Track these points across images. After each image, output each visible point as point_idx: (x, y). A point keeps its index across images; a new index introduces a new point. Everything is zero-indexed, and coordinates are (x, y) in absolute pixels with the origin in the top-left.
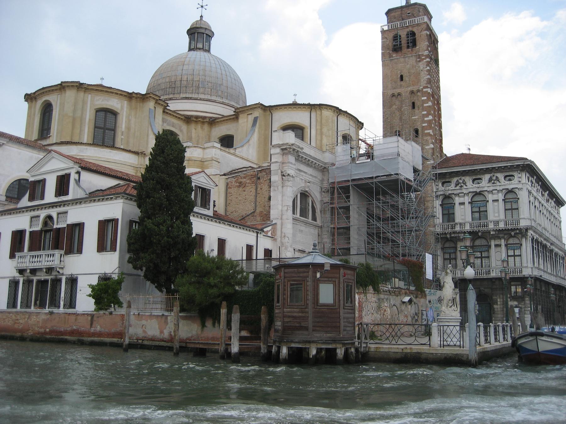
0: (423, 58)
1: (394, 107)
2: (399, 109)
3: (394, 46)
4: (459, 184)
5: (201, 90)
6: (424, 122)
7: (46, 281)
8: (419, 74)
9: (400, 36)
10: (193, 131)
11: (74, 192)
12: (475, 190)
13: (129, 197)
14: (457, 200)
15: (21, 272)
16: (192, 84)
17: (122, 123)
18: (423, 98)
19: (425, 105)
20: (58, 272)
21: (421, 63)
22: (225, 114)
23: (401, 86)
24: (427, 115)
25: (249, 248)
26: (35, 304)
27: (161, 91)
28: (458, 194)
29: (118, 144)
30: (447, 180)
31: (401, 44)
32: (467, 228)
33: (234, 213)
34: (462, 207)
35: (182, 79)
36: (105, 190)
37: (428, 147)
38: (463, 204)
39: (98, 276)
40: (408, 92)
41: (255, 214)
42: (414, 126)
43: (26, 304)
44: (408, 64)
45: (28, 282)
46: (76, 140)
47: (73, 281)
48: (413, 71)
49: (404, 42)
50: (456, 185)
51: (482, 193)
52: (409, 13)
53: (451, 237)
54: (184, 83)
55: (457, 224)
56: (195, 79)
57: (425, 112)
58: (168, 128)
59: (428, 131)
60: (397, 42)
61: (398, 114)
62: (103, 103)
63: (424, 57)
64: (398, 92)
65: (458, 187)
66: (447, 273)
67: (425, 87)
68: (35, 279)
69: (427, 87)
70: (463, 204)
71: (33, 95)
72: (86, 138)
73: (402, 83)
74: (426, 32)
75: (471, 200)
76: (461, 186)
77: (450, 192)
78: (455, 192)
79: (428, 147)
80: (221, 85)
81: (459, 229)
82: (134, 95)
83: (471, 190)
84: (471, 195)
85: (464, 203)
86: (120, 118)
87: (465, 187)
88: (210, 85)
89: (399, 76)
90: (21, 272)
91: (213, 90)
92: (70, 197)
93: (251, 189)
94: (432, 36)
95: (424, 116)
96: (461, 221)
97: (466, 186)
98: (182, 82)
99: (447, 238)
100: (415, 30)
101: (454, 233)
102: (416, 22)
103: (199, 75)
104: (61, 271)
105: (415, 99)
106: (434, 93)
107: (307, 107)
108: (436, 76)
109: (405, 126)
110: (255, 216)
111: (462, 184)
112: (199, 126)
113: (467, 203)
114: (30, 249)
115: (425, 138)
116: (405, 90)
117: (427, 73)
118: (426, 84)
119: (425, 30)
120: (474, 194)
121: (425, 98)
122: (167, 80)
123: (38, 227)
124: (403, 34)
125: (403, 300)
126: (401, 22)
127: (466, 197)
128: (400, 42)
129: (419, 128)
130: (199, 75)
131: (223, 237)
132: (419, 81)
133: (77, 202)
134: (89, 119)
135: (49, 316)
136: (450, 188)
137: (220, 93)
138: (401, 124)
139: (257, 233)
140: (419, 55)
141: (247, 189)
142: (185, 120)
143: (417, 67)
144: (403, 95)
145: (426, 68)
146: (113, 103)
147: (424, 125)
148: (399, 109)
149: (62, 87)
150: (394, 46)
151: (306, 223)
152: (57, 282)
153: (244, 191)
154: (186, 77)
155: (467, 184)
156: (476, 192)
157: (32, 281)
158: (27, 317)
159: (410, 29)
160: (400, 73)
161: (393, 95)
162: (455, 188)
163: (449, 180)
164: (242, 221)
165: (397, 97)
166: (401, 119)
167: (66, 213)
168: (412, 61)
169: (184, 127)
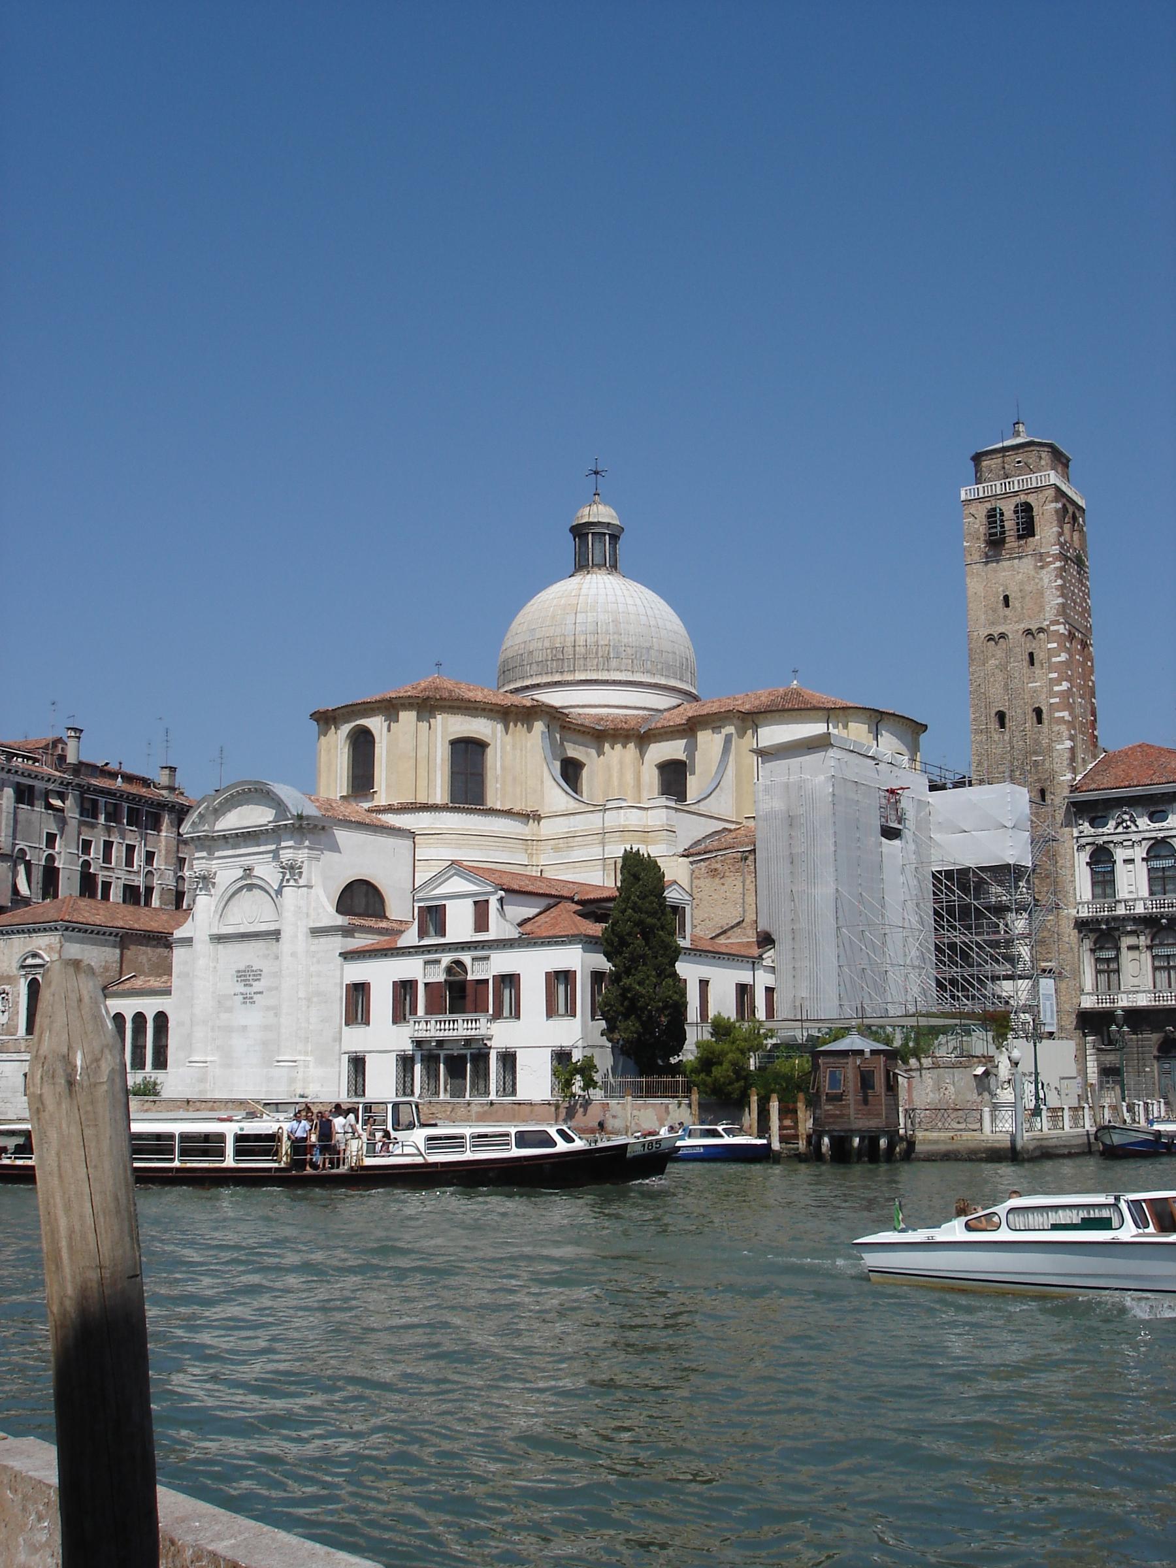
0: (1048, 560)
1: (992, 662)
3: (991, 535)
4: (1122, 823)
5: (614, 663)
6: (1052, 694)
7: (465, 1056)
8: (1042, 594)
9: (1002, 514)
11: (498, 928)
12: (1154, 834)
13: (590, 943)
14: (1120, 854)
15: (418, 1043)
16: (597, 653)
17: (495, 761)
18: (1050, 646)
19: (1054, 660)
20: (486, 1044)
21: (1044, 571)
22: (661, 708)
23: (1005, 617)
24: (1058, 682)
26: (446, 1089)
27: (534, 667)
28: (1122, 843)
29: (493, 799)
30: (1099, 814)
31: (1003, 533)
32: (1140, 909)
33: (707, 921)
34: (1130, 867)
35: (577, 644)
36: (533, 918)
37: (1063, 746)
38: (1130, 861)
39: (550, 1049)
40: (1021, 632)
41: (744, 925)
42: (1034, 703)
44: (1018, 573)
46: (422, 799)
47: (508, 1060)
48: (1028, 588)
49: (1009, 525)
50: (1118, 824)
51: (1168, 840)
52: (1019, 462)
53: (1108, 929)
54: (581, 650)
55: (1119, 901)
56: (601, 643)
57: (1055, 675)
59: (1061, 714)
60: (996, 527)
61: (1000, 676)
63: (1051, 559)
64: (1000, 631)
65: (1120, 829)
66: (1001, 1052)
68: (442, 1053)
69: (1057, 623)
70: (1130, 861)
71: (330, 714)
72: (440, 794)
73: (1007, 611)
74: (1053, 505)
75: (1147, 853)
76: (1128, 827)
77: (1106, 838)
78: (1116, 838)
79: (1063, 746)
80: (649, 649)
81: (1123, 912)
82: (513, 709)
83: (1147, 835)
84: (1146, 845)
85: (1133, 860)
86: (489, 751)
87: (1134, 828)
88: (629, 651)
89: (1002, 598)
90: (418, 1043)
91: (635, 662)
93: (735, 883)
94: (1068, 505)
96: (1127, 896)
97: (1137, 826)
98: (577, 648)
99: (1101, 930)
100: (1031, 499)
101: (1115, 918)
102: (1034, 485)
103: (607, 633)
104: (489, 1043)
105: (1031, 645)
106: (1073, 630)
107: (820, 713)
108: (1080, 590)
109: (1014, 702)
110: (744, 928)
111: (1129, 823)
112: (618, 747)
113: (1138, 860)
114: (429, 1011)
115: (1056, 728)
117: (1058, 593)
118: (1056, 616)
119: (1052, 502)
120: (1152, 842)
121: (1055, 645)
122: (547, 644)
123: (438, 976)
124: (1008, 508)
125: (975, 1073)
126: (1003, 481)
127: (1137, 848)
128: (1002, 527)
129: (1043, 708)
130: (607, 633)
131: (705, 976)
132: (1042, 609)
134: (442, 760)
135: (486, 1108)
136: (1105, 830)
137: (649, 665)
138: (1006, 698)
139: (754, 963)
140: (1041, 554)
141: (729, 881)
142: (593, 735)
143: (1037, 580)
144: (1010, 637)
145: (1056, 581)
147: (1052, 701)
148: (1003, 667)
150: (991, 535)
152: (481, 1058)
153: (723, 884)
154: (583, 638)
155: (1137, 823)
156: (1156, 838)
157: (439, 1055)
158: (450, 1109)
159: (1023, 498)
160: (1004, 591)
161: (990, 638)
162: (1117, 831)
163: (1104, 814)
164: (722, 940)
165: (996, 643)
166: (1006, 687)
167: (487, 958)
168: (1027, 565)
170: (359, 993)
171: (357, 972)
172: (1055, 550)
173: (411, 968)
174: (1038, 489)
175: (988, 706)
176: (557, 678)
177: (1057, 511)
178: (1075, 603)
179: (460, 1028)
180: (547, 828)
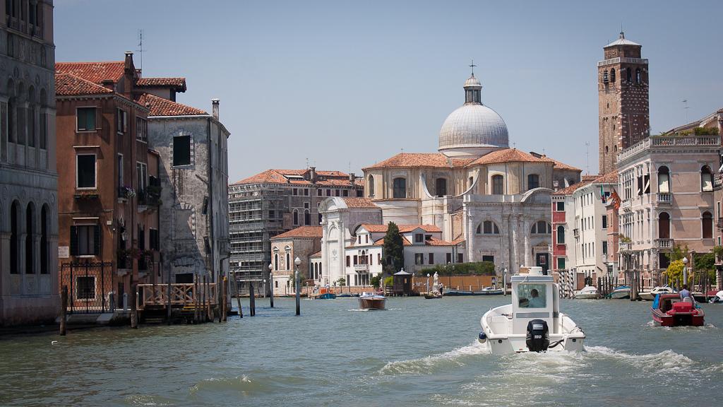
2: (607, 129)
10: (455, 174)
24: (619, 136)
25: (449, 255)
43: (360, 284)
45: (360, 276)
54: (455, 137)
58: (439, 177)
62: (398, 174)
67: (619, 114)
72: (391, 196)
92: (368, 244)
95: (619, 136)
108: (638, 98)
112: (459, 172)
116: (609, 116)
124: (609, 70)
133: (370, 246)
146: (402, 174)
148: (607, 129)
149: (375, 169)
151: (489, 237)
169: (450, 173)
170: (348, 257)
171: (349, 253)
172: (620, 87)
173: (356, 252)
174: (615, 65)
175: (604, 144)
176: (449, 147)
177: (621, 72)
178: (634, 104)
179: (363, 268)
180: (424, 204)
